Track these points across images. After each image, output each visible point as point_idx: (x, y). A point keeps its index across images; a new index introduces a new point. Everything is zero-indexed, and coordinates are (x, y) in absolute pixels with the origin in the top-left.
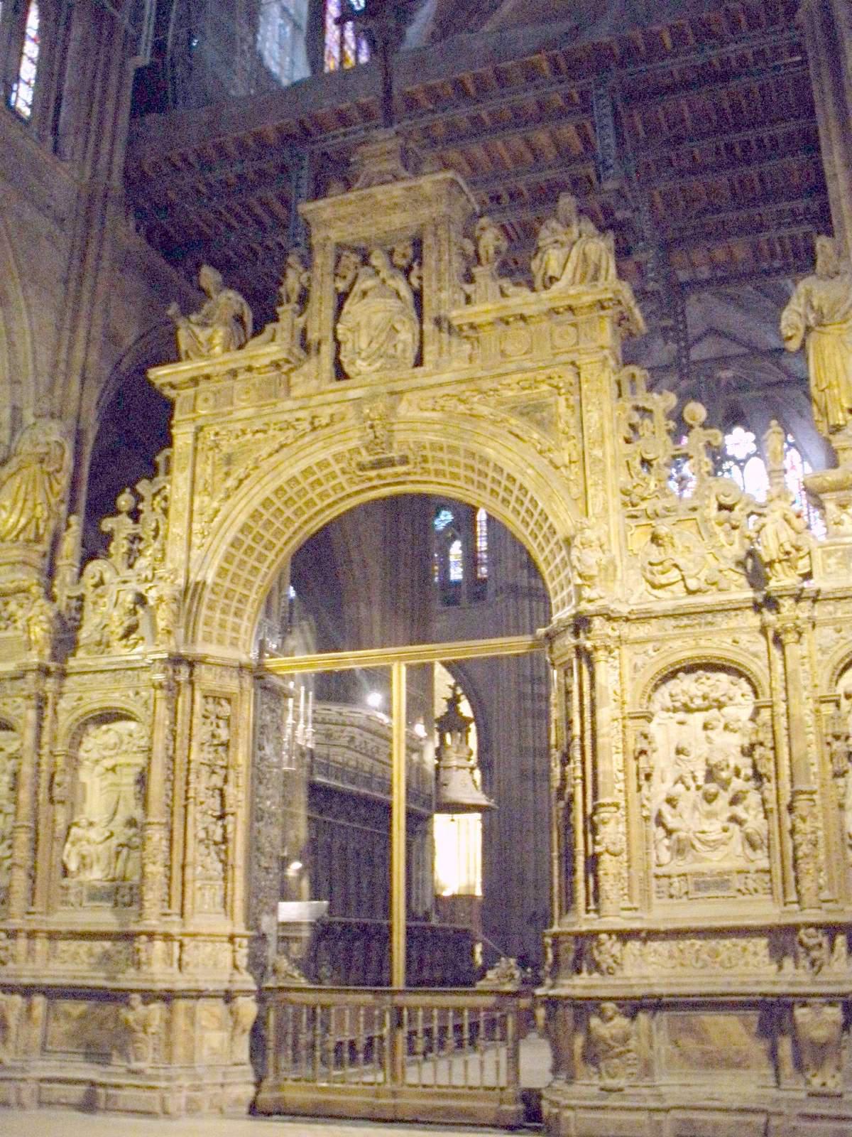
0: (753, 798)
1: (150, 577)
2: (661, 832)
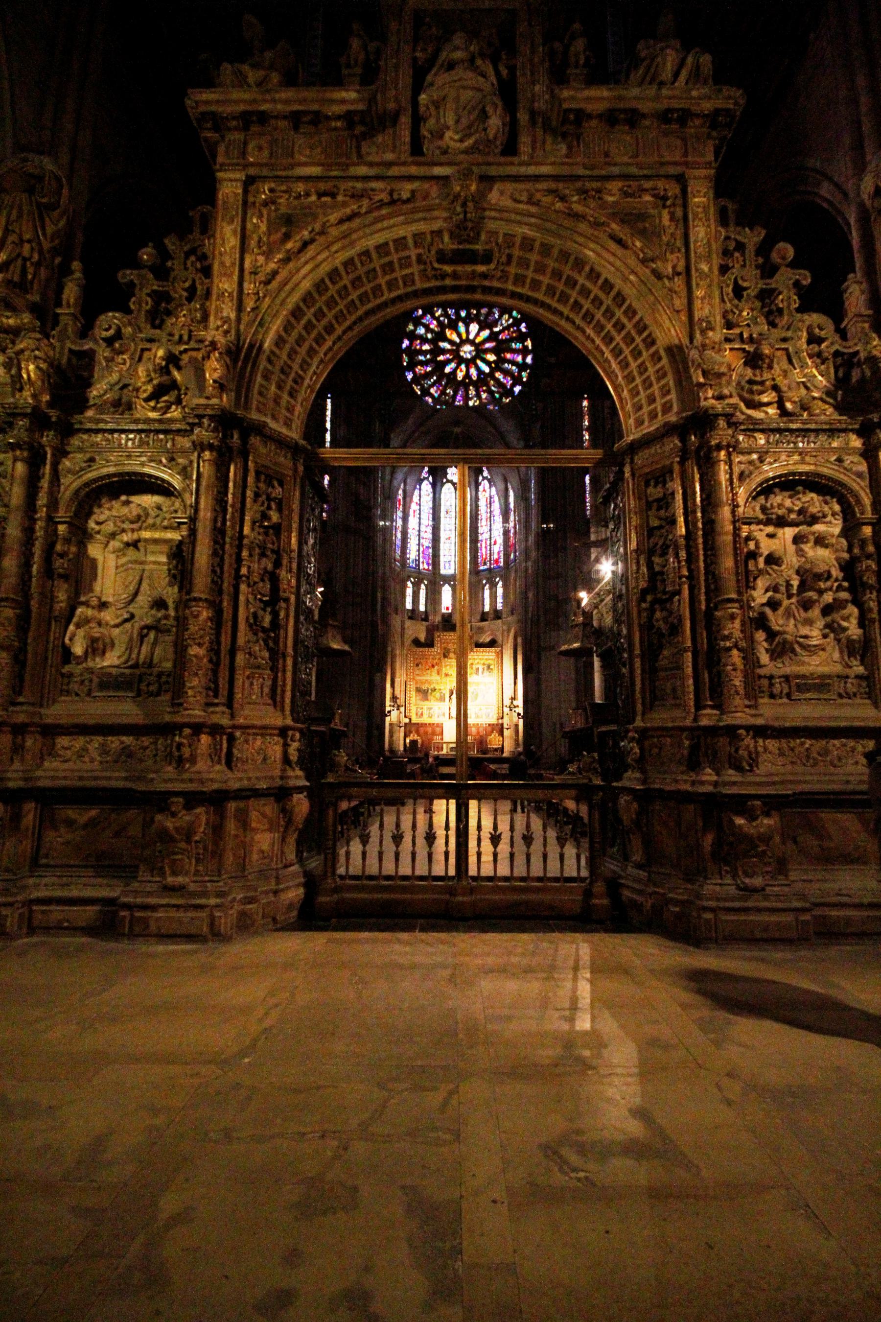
1: (186, 338)
2: (760, 636)
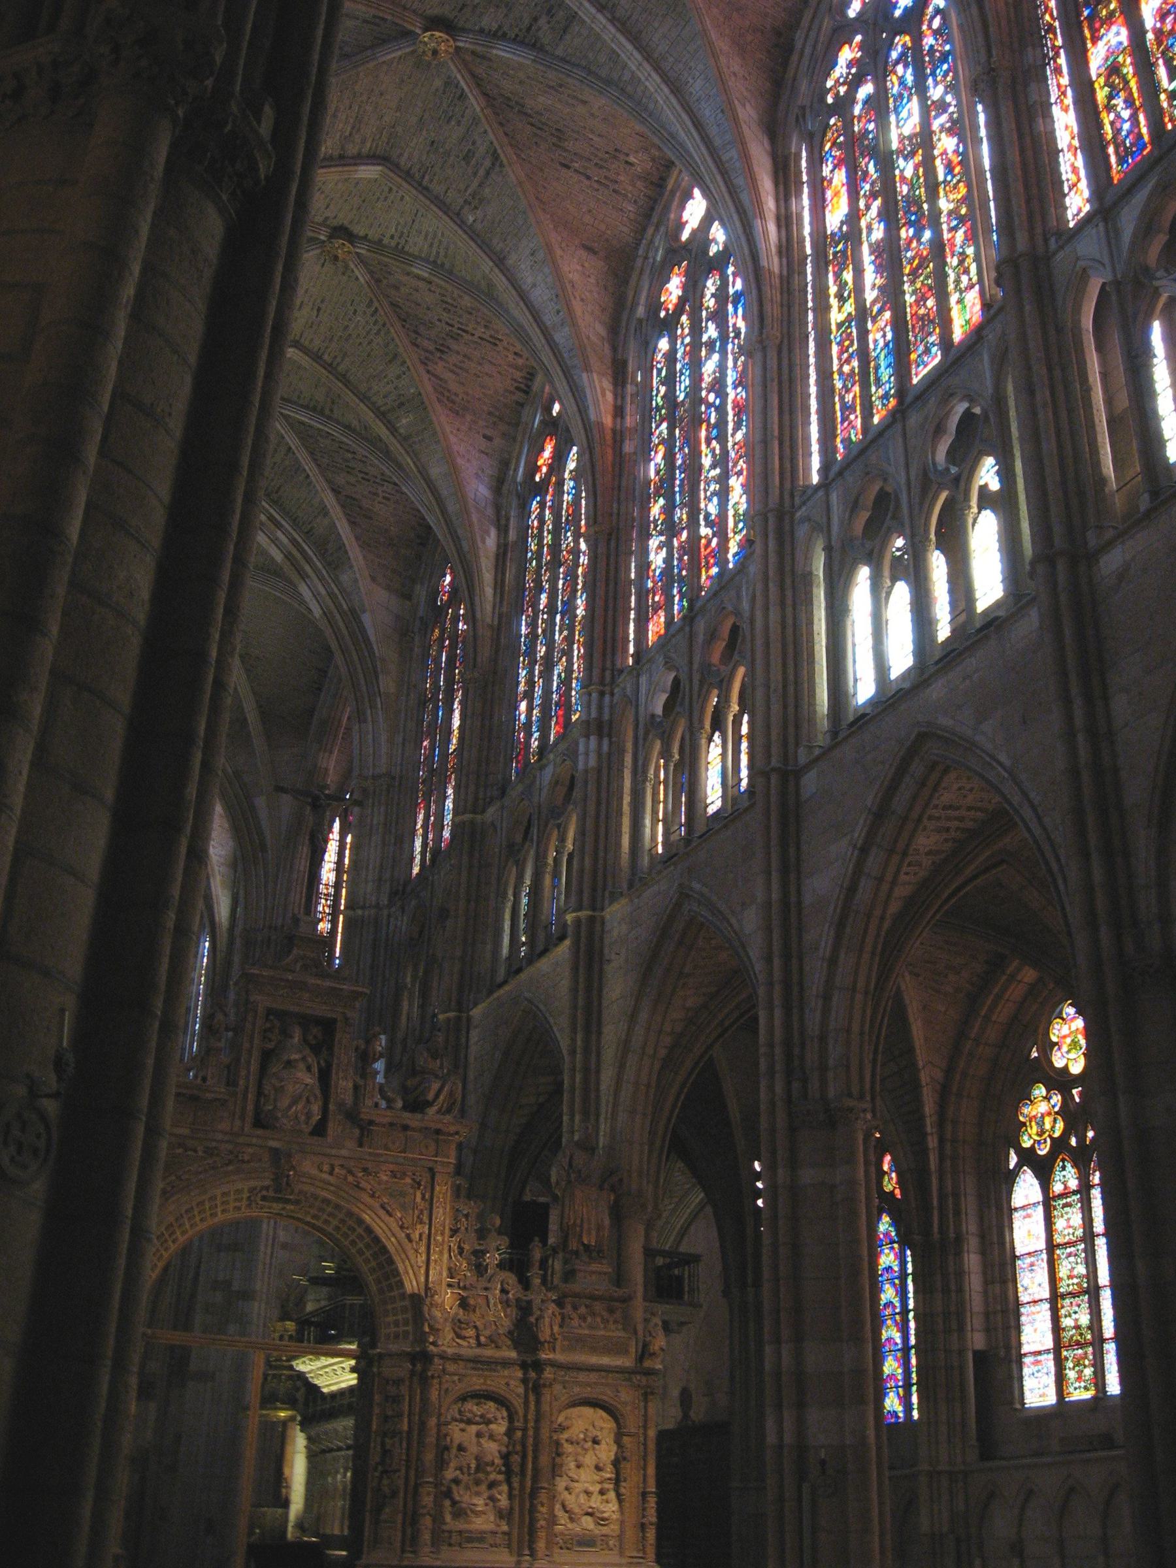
0: (505, 1488)
2: (447, 1503)
